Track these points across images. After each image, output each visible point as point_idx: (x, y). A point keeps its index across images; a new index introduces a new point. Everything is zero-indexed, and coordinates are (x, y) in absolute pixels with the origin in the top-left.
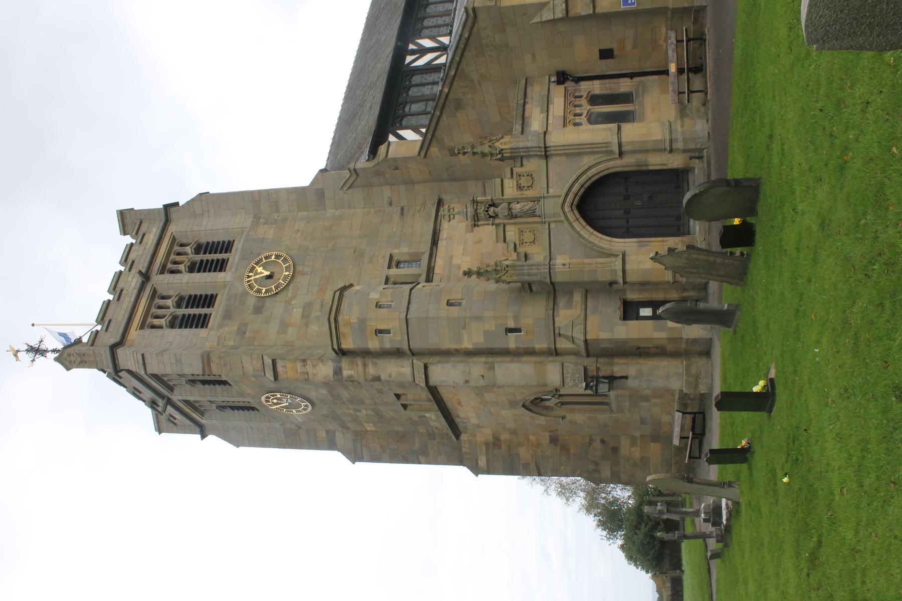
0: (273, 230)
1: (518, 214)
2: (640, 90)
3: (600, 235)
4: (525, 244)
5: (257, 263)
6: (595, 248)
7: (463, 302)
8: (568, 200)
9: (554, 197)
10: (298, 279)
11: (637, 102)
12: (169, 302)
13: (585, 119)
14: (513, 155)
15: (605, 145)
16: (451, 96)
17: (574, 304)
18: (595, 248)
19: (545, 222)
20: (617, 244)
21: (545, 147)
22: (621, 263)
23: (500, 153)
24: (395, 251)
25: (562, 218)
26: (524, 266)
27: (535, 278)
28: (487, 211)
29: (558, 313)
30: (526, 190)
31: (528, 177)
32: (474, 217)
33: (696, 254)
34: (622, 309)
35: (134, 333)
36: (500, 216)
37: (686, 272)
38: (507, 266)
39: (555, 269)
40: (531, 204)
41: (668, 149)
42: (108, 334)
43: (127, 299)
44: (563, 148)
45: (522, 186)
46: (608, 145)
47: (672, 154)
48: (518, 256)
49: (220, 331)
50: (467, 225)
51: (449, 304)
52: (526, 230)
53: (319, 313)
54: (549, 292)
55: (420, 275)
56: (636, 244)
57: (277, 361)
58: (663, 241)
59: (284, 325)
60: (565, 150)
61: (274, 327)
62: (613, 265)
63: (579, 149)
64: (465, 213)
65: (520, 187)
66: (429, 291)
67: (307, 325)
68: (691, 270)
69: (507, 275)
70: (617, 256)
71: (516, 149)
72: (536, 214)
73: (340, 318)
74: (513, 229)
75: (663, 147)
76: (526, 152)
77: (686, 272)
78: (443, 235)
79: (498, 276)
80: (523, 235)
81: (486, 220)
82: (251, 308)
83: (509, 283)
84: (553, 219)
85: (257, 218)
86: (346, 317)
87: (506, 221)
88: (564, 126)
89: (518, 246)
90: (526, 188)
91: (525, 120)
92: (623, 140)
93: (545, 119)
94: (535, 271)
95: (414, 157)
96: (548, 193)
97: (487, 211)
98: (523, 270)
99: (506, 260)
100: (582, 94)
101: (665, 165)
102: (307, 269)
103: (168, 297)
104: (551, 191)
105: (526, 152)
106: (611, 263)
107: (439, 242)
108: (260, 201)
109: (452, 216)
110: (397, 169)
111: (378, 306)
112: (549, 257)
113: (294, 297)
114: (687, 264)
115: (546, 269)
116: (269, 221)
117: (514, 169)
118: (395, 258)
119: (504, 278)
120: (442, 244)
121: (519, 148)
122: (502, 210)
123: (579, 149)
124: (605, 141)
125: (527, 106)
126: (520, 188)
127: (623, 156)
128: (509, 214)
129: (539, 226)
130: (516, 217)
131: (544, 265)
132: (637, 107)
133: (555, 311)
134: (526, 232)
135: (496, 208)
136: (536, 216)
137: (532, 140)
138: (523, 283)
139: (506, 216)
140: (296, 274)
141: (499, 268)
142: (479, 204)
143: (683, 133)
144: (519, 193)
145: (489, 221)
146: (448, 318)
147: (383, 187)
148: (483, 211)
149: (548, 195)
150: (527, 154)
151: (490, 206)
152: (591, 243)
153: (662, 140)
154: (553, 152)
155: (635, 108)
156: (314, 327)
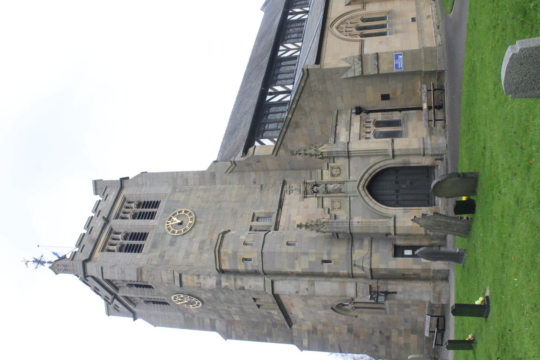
0: (184, 195)
2: (406, 119)
3: (380, 205)
4: (335, 209)
5: (173, 215)
6: (377, 212)
7: (297, 243)
8: (361, 184)
9: (353, 181)
10: (197, 225)
11: (403, 126)
12: (120, 236)
13: (372, 135)
14: (329, 155)
15: (384, 151)
16: (293, 120)
17: (364, 246)
18: (377, 212)
19: (347, 196)
20: (391, 211)
21: (348, 152)
22: (393, 222)
23: (321, 155)
24: (256, 211)
25: (358, 194)
26: (334, 222)
27: (340, 230)
28: (312, 189)
29: (354, 252)
31: (338, 169)
32: (305, 192)
33: (439, 218)
34: (393, 250)
35: (97, 254)
36: (320, 192)
37: (433, 229)
38: (324, 222)
39: (353, 225)
40: (339, 185)
41: (422, 154)
42: (82, 254)
44: (359, 152)
45: (334, 174)
46: (386, 151)
47: (425, 157)
48: (330, 216)
49: (149, 255)
50: (300, 197)
51: (288, 244)
52: (336, 201)
53: (209, 247)
54: (349, 239)
55: (271, 226)
56: (402, 211)
57: (182, 275)
58: (419, 209)
59: (188, 254)
60: (360, 153)
61: (182, 254)
62: (388, 223)
63: (368, 153)
64: (299, 189)
65: (332, 175)
66: (276, 236)
67: (201, 254)
68: (436, 228)
69: (323, 227)
70: (391, 218)
71: (331, 152)
72: (342, 191)
73: (222, 251)
75: (419, 153)
76: (336, 154)
77: (433, 229)
78: (286, 202)
79: (318, 228)
81: (312, 194)
82: (169, 242)
83: (325, 232)
84: (352, 195)
85: (174, 189)
86: (225, 250)
87: (324, 195)
88: (360, 139)
89: (330, 210)
90: (336, 175)
91: (337, 135)
92: (395, 148)
93: (349, 135)
94: (340, 226)
95: (270, 155)
96: (349, 179)
97: (312, 189)
98: (333, 225)
99: (323, 218)
100: (371, 120)
101: (420, 163)
102: (202, 220)
104: (351, 177)
105: (336, 154)
106: (387, 222)
107: (283, 206)
108: (177, 178)
109: (291, 191)
110: (259, 162)
111: (245, 244)
112: (349, 217)
113: (194, 236)
114: (433, 224)
115: (348, 224)
116: (182, 190)
117: (329, 164)
118: (256, 215)
119: (321, 229)
120: (284, 207)
121: (332, 152)
122: (321, 188)
123: (368, 153)
124: (384, 149)
125: (338, 127)
126: (332, 175)
127: (395, 158)
129: (343, 198)
130: (330, 193)
131: (346, 222)
132: (403, 129)
133: (352, 250)
135: (318, 187)
136: (342, 193)
137: (340, 147)
138: (333, 233)
140: (197, 223)
141: (319, 223)
142: (308, 185)
143: (431, 144)
144: (332, 178)
145: (314, 195)
146: (287, 252)
147: (251, 172)
148: (310, 189)
149: (350, 180)
150: (337, 155)
151: (314, 186)
152: (375, 209)
153: (418, 148)
154: (353, 155)
155: (402, 129)
156: (205, 255)
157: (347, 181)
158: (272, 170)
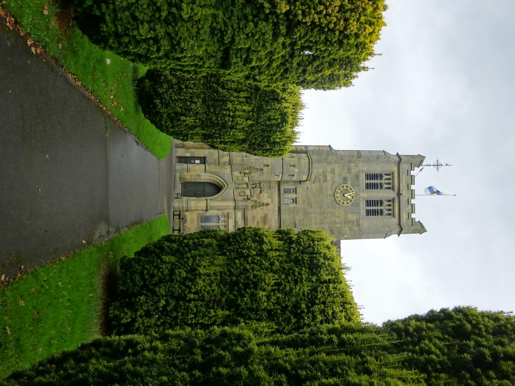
12: (386, 186)
35: (395, 169)
42: (406, 168)
43: (404, 185)
103: (386, 188)
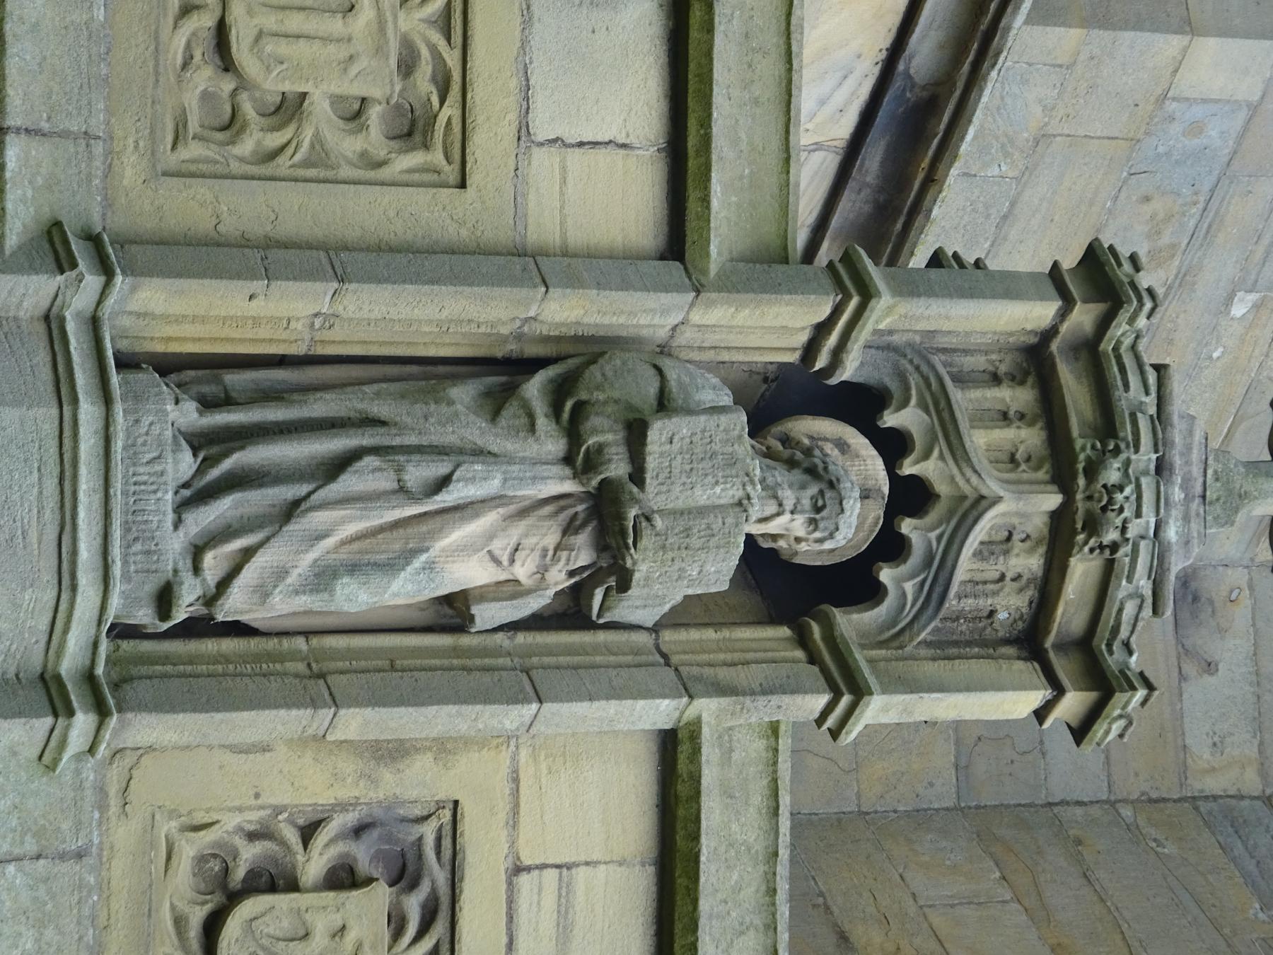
1: (475, 430)
30: (308, 833)
72: (188, 415)
74: (543, 162)
80: (407, 67)
128: (636, 433)
134: (355, 114)
139: (664, 404)
148: (979, 504)
157: (60, 707)
158: (921, 818)
